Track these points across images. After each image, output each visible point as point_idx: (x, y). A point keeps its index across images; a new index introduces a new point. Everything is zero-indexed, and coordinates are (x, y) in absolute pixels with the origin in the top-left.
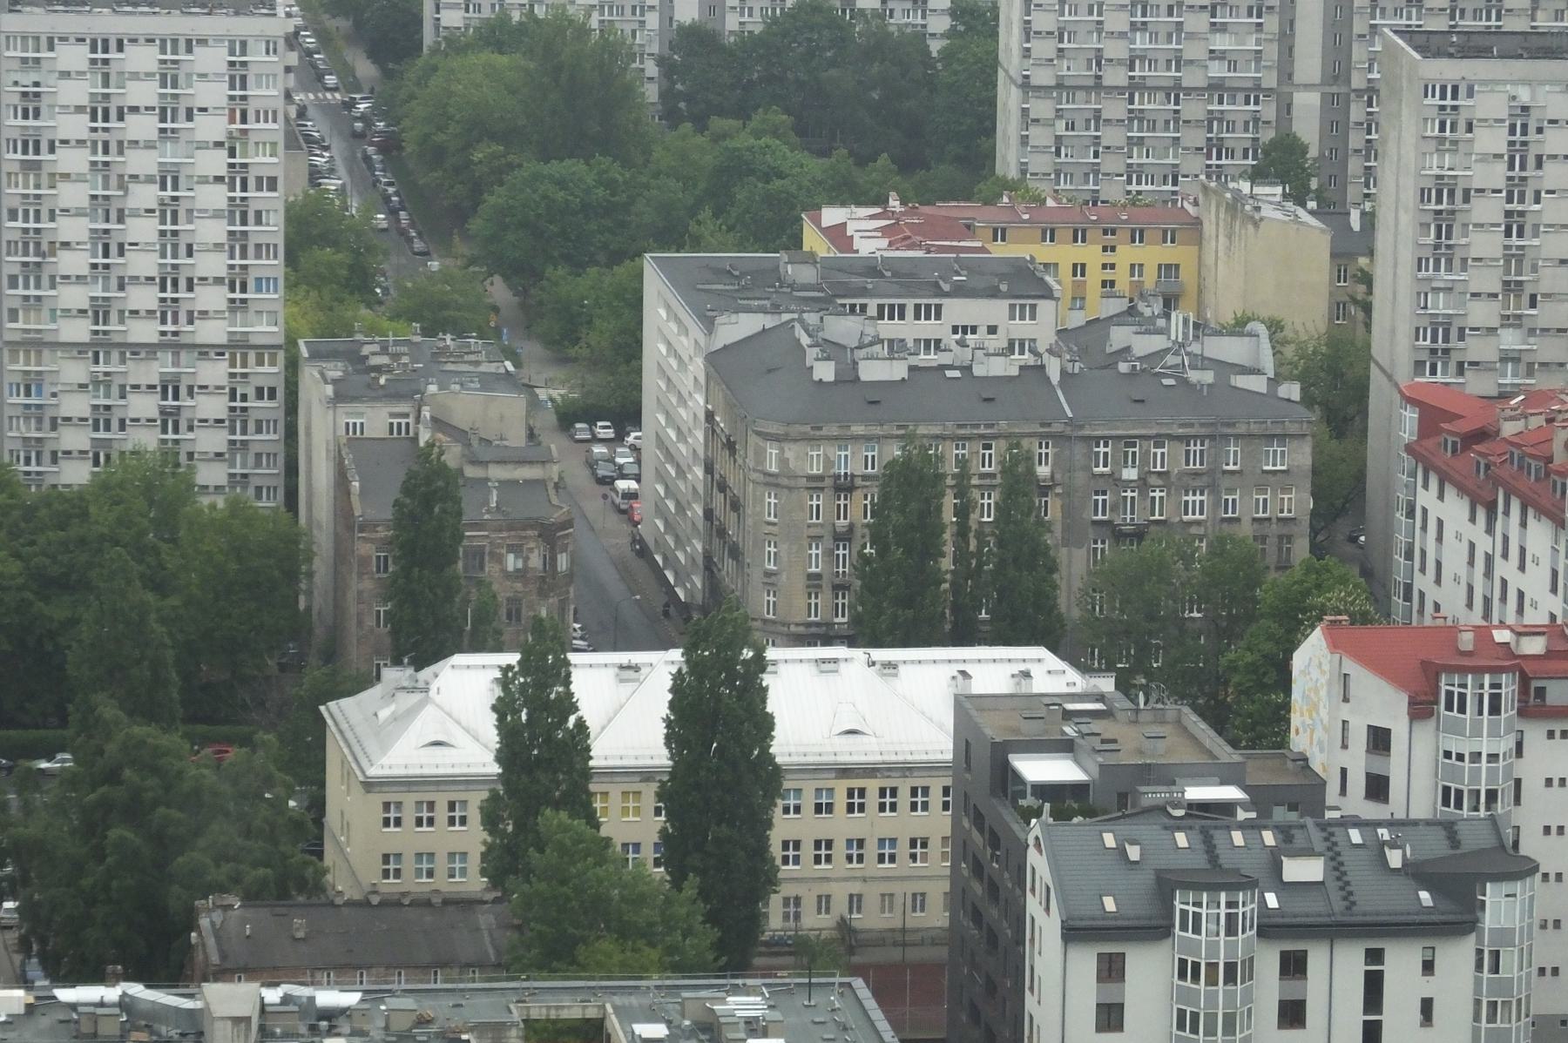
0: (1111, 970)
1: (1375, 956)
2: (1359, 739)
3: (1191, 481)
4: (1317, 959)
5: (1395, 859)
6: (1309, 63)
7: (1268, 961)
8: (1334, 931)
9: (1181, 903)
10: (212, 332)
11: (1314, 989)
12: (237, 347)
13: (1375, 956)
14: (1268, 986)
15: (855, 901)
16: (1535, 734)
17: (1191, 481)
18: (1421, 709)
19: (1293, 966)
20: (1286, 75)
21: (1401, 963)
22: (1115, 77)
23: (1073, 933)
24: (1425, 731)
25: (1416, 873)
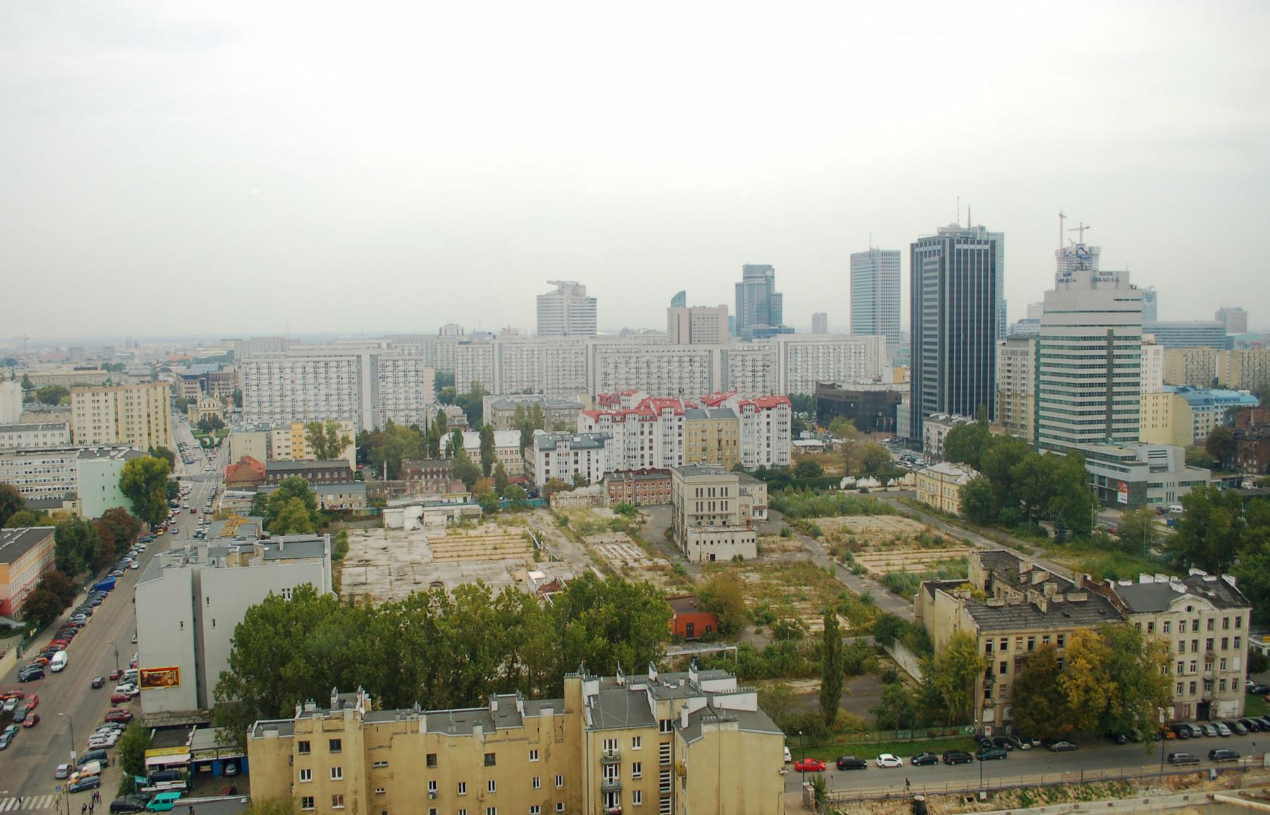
0: (547, 455)
1: (589, 452)
2: (587, 427)
3: (566, 416)
4: (580, 452)
5: (592, 438)
6: (591, 383)
7: (572, 453)
8: (582, 448)
9: (558, 444)
10: (413, 407)
11: (579, 458)
12: (417, 410)
13: (589, 452)
14: (572, 458)
15: (512, 469)
16: (614, 425)
17: (566, 416)
18: (597, 421)
19: (576, 454)
20: (587, 385)
21: (593, 452)
22: (561, 386)
23: (541, 450)
24: (597, 425)
25: (595, 440)
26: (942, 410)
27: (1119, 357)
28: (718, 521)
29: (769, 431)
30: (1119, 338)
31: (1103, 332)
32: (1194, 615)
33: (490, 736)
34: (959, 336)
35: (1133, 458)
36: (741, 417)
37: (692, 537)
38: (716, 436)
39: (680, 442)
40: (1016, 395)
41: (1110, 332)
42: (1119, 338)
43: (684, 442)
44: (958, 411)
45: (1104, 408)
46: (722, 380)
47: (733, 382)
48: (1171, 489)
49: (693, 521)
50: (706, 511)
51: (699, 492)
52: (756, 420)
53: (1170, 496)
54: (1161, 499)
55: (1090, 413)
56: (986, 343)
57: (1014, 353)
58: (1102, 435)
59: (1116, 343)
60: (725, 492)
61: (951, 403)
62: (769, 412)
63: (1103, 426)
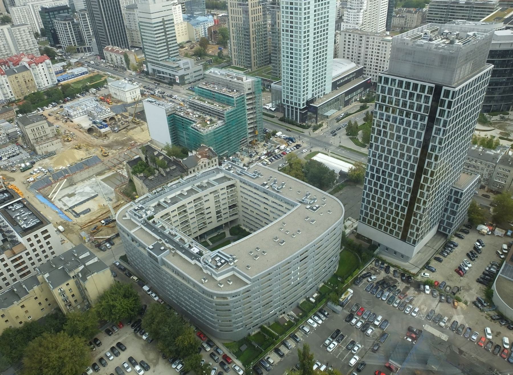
26: (109, 45)
27: (167, 28)
28: (44, 138)
29: (46, 78)
30: (166, 21)
31: (160, 20)
32: (204, 163)
33: (20, 301)
34: (108, 14)
35: (178, 67)
36: (31, 69)
37: (37, 148)
38: (23, 79)
39: (8, 86)
40: (134, 30)
41: (163, 19)
42: (166, 21)
43: (10, 86)
44: (115, 45)
45: (166, 47)
46: (11, 37)
47: (18, 41)
48: (192, 75)
49: (34, 141)
50: (38, 136)
51: (33, 130)
52: (38, 69)
53: (192, 77)
54: (189, 79)
55: (159, 37)
56: (117, 8)
57: (129, 14)
58: (167, 57)
59: (166, 23)
60: (43, 127)
61: (111, 41)
62: (42, 64)
63: (167, 54)
